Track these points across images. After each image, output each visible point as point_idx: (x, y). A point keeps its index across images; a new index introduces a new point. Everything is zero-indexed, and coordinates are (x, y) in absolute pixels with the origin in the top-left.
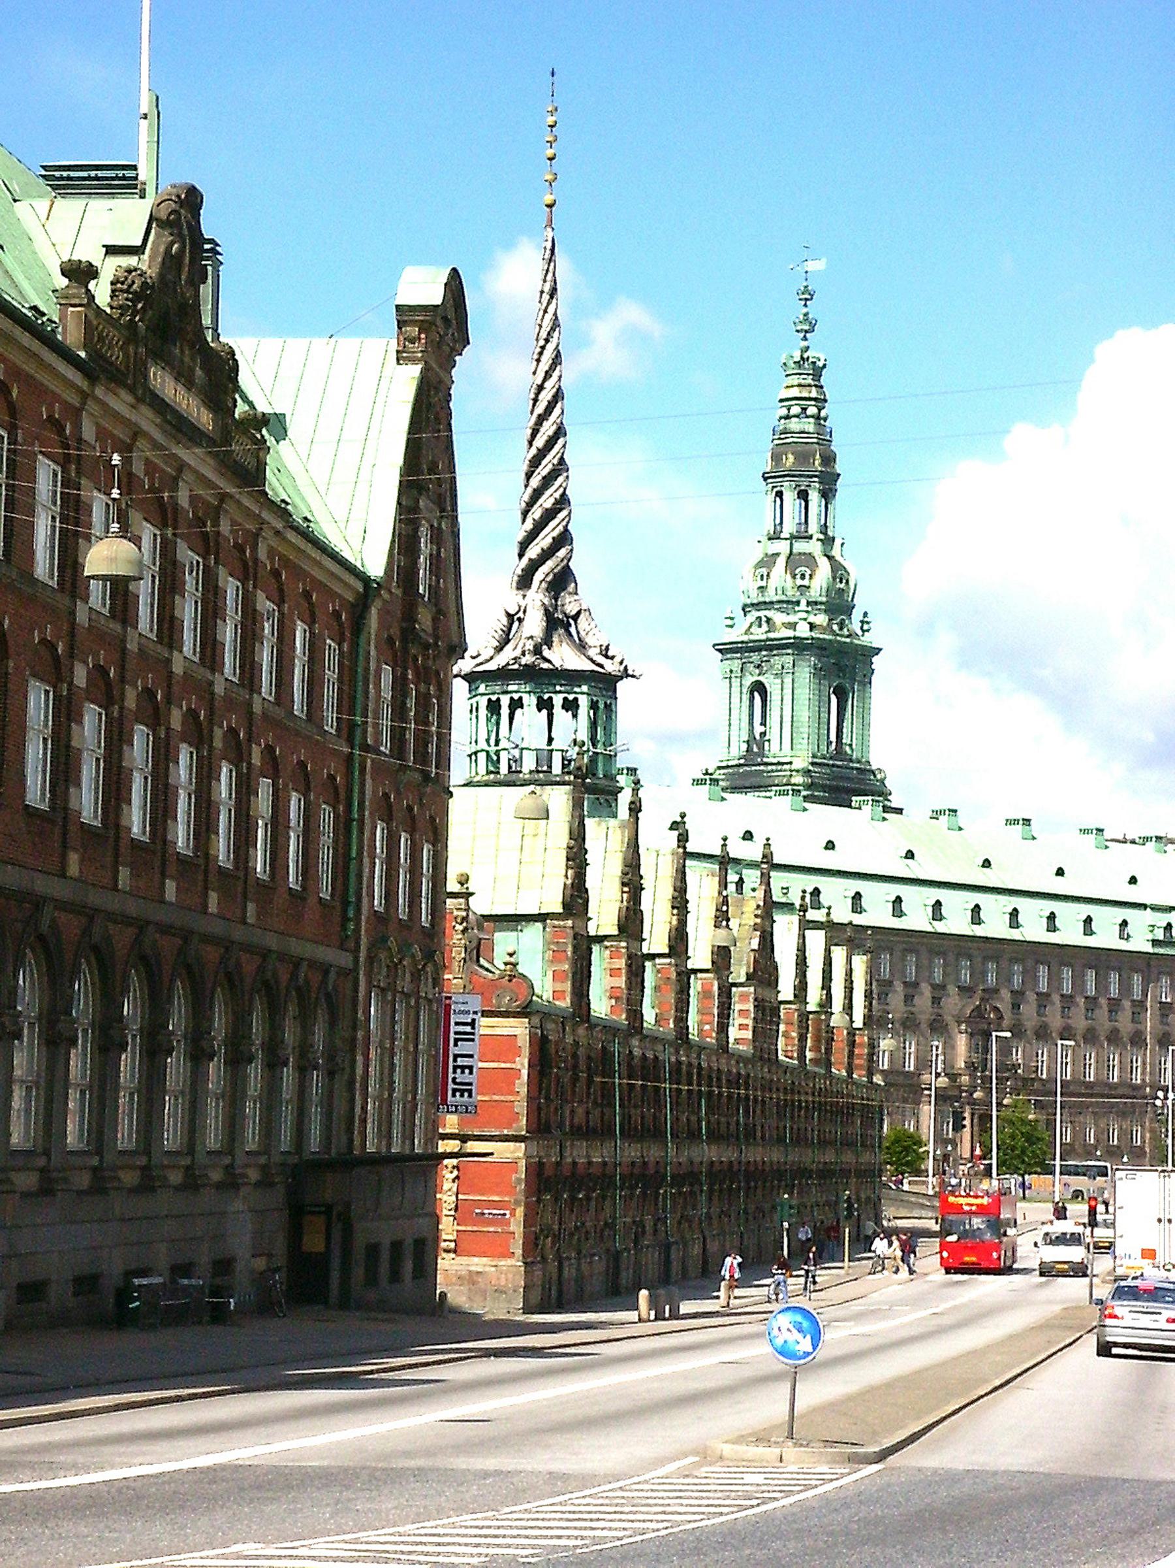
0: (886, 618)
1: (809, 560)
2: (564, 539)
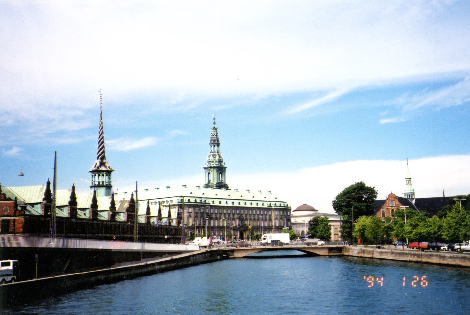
0: (226, 163)
1: (216, 155)
2: (104, 152)
